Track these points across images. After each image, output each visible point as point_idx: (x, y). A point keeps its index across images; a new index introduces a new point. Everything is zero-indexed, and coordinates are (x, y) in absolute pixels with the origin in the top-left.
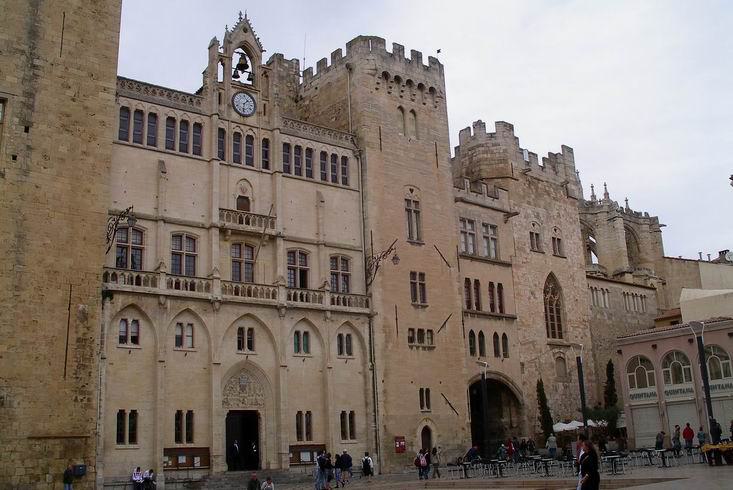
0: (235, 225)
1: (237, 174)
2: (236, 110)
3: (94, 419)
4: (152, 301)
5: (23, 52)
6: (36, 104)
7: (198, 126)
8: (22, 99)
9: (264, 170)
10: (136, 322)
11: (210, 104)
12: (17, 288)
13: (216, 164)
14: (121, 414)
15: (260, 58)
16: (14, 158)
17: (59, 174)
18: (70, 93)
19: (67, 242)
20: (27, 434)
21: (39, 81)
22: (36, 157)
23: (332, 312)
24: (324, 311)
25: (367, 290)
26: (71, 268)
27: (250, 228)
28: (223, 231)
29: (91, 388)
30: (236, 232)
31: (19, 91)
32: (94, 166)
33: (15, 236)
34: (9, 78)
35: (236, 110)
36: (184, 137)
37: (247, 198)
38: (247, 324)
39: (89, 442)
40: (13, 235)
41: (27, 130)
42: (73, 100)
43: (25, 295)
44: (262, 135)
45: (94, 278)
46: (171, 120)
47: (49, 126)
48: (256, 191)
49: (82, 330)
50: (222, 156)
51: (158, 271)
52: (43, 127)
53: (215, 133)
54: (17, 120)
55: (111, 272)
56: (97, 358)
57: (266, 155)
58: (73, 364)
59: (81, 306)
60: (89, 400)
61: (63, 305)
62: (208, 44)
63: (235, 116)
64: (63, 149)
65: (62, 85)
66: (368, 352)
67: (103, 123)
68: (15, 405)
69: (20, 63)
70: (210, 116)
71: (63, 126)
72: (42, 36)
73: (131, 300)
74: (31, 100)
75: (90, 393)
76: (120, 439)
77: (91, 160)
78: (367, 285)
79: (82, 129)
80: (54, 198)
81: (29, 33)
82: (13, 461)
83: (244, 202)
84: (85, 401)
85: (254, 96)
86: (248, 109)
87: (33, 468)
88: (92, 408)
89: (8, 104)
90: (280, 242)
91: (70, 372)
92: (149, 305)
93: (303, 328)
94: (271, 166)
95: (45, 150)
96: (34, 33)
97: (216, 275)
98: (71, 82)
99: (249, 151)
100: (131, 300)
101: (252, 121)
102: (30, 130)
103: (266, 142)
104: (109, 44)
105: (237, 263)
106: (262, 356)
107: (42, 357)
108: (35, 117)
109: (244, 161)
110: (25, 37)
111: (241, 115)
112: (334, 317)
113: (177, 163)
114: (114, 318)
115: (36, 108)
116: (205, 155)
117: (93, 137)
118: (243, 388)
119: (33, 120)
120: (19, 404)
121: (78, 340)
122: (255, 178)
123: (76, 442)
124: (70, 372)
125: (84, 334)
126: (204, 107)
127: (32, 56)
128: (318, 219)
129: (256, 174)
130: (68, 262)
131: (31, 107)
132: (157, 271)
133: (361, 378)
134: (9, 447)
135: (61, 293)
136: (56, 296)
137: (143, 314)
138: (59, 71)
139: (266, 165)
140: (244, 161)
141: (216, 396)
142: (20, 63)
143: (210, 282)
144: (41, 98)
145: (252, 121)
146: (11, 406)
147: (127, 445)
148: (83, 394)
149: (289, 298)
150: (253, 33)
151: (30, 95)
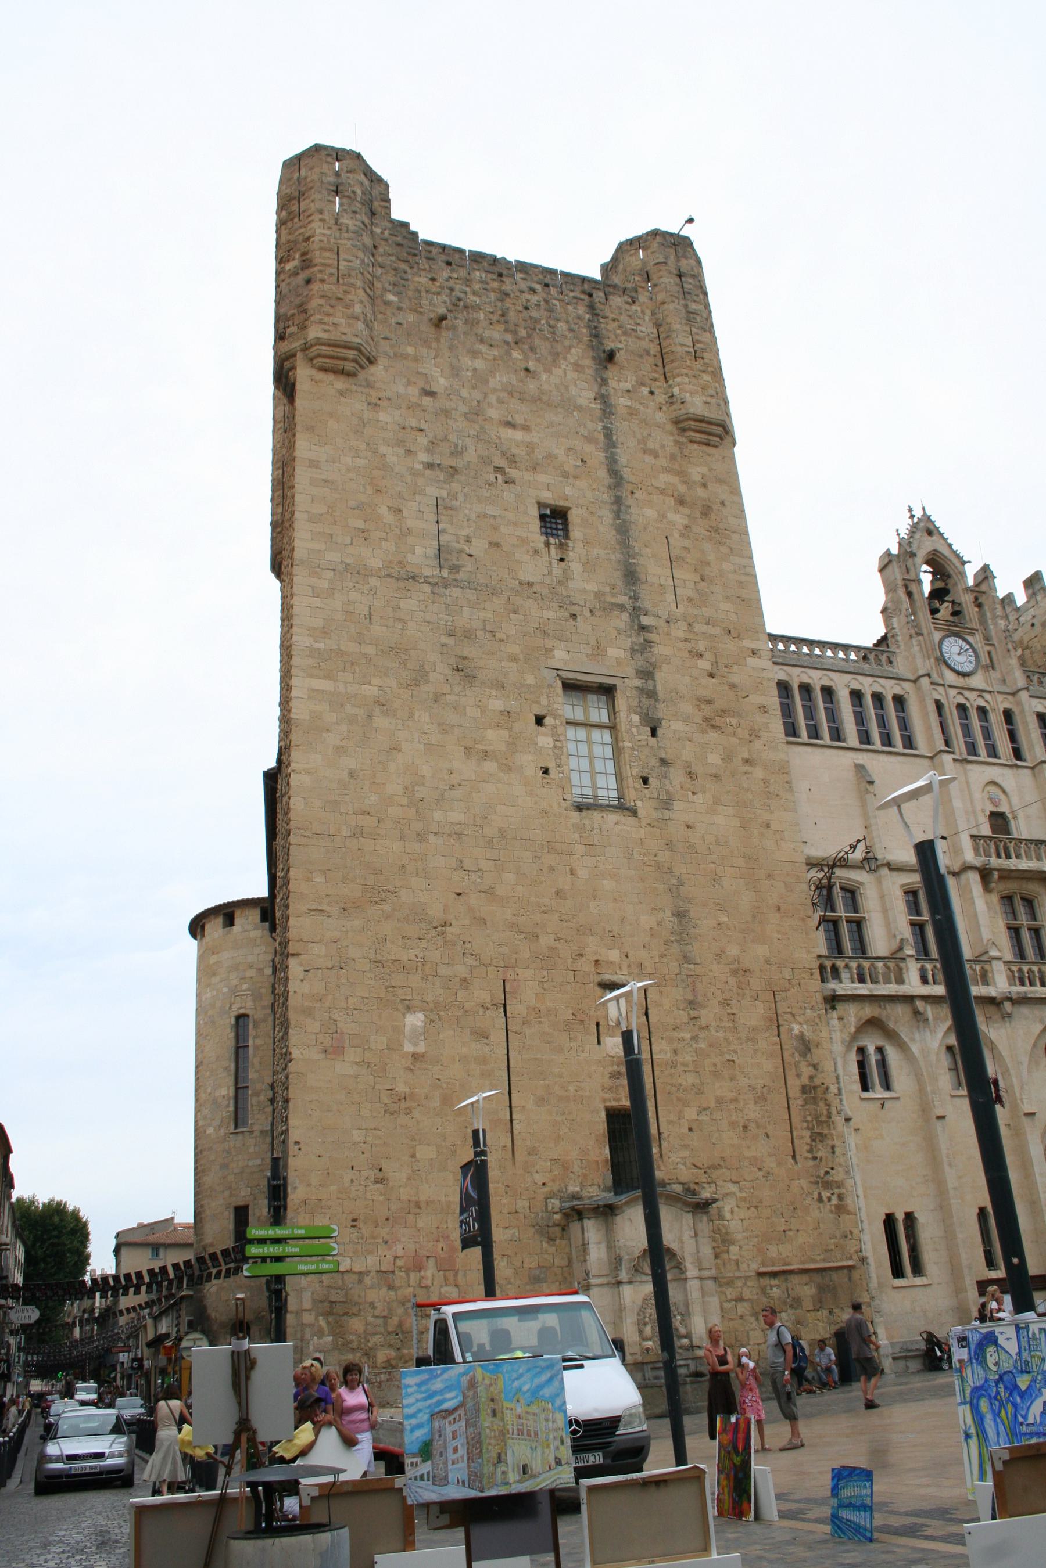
0: (1000, 861)
1: (980, 774)
2: (949, 666)
3: (856, 1232)
5: (622, 607)
6: (659, 688)
7: (899, 701)
8: (638, 683)
9: (1019, 763)
10: (880, 1050)
11: (910, 659)
12: (692, 1004)
13: (947, 758)
14: (889, 1221)
15: (963, 575)
16: (645, 781)
17: (717, 802)
18: (704, 665)
19: (754, 917)
20: (754, 1266)
21: (655, 650)
22: (677, 776)
26: (767, 961)
27: (1025, 864)
28: (985, 874)
29: (838, 1175)
30: (1007, 875)
31: (630, 671)
32: (765, 782)
33: (673, 915)
34: (614, 652)
35: (949, 666)
36: (882, 721)
37: (1002, 815)
39: (856, 1275)
40: (667, 915)
41: (654, 733)
42: (712, 676)
43: (707, 1015)
44: (998, 705)
45: (806, 976)
46: (856, 695)
47: (686, 720)
48: (1015, 800)
49: (806, 1071)
50: (947, 743)
51: (899, 955)
52: (677, 726)
53: (932, 708)
54: (636, 718)
55: (828, 964)
56: (839, 1120)
57: (1012, 736)
58: (804, 1136)
59: (796, 1029)
60: (840, 1197)
61: (768, 1028)
62: (876, 566)
63: (950, 677)
64: (714, 758)
65: (690, 652)
67: (763, 709)
68: (728, 1216)
69: (622, 626)
70: (914, 681)
71: (706, 719)
72: (642, 577)
73: (869, 1011)
74: (650, 682)
75: (839, 1185)
76: (897, 1271)
77: (758, 773)
79: (734, 721)
80: (718, 843)
81: (625, 576)
82: (741, 1317)
83: (999, 820)
84: (835, 1201)
85: (969, 638)
86: (964, 661)
88: (849, 1213)
89: (619, 694)
91: (802, 1148)
92: (897, 1016)
94: (1026, 752)
95: (688, 765)
96: (631, 576)
97: (994, 953)
98: (701, 646)
99: (987, 733)
100: (869, 1011)
101: (977, 681)
102: (660, 731)
103: (1008, 715)
104: (743, 578)
105: (1015, 932)
107: (752, 1125)
108: (662, 711)
109: (982, 750)
110: (620, 583)
111: (959, 673)
113: (878, 764)
115: (661, 695)
116: (923, 748)
117: (754, 734)
119: (660, 715)
120: (732, 1212)
121: (804, 1089)
122: (1008, 778)
123: (834, 1279)
124: (802, 1148)
125: (811, 1078)
126: (901, 667)
127: (636, 612)
129: (1007, 771)
130: (761, 951)
131: (652, 694)
132: (896, 956)
135: (760, 1009)
136: (753, 1015)
137: (891, 1035)
138: (679, 631)
139: (1018, 754)
140: (982, 750)
142: (622, 626)
143: (987, 967)
144: (663, 679)
145: (977, 681)
146: (721, 1217)
147: (910, 1280)
148: (828, 1185)
150: (941, 534)
151: (647, 674)
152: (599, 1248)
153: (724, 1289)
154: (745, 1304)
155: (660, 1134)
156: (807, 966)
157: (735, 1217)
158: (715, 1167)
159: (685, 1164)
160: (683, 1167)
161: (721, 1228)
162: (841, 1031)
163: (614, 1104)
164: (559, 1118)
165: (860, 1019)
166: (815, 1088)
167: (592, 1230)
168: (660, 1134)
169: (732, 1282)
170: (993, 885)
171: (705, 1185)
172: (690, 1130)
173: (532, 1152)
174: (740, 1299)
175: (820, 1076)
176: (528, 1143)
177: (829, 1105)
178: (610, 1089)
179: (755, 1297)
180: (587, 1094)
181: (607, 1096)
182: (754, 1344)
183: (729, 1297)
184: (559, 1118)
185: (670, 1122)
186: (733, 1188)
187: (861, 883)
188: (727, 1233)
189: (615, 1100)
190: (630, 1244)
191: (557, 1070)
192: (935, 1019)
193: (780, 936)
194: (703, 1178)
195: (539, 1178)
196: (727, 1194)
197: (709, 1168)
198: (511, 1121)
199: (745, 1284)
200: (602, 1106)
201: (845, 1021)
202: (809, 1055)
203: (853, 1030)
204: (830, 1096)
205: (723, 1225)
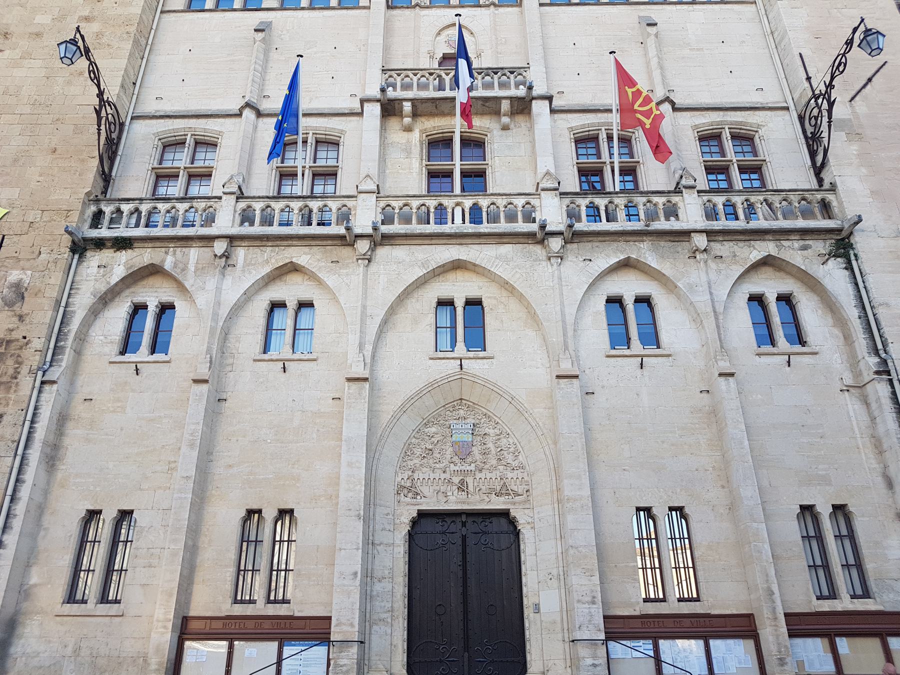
4: (194, 253)
23: (711, 234)
24: (685, 234)
25: (820, 181)
38: (460, 288)
56: (26, 383)
66: (857, 325)
78: (818, 170)
90: (540, 108)
93: (629, 287)
106: (515, 358)
112: (722, 248)
114: (106, 299)
118: (463, 452)
128: (648, 63)
133: (851, 404)
137: (181, 287)
141: (350, 464)
149: (573, 215)
156: (65, 207)
162: (96, 280)
165: (132, 266)
166: (9, 342)
170: (407, 120)
175: (21, 327)
177: (20, 363)
187: (220, 133)
192: (247, 264)
193: (40, 179)
201: (108, 269)
202: (19, 304)
203: (115, 279)
204: (27, 353)
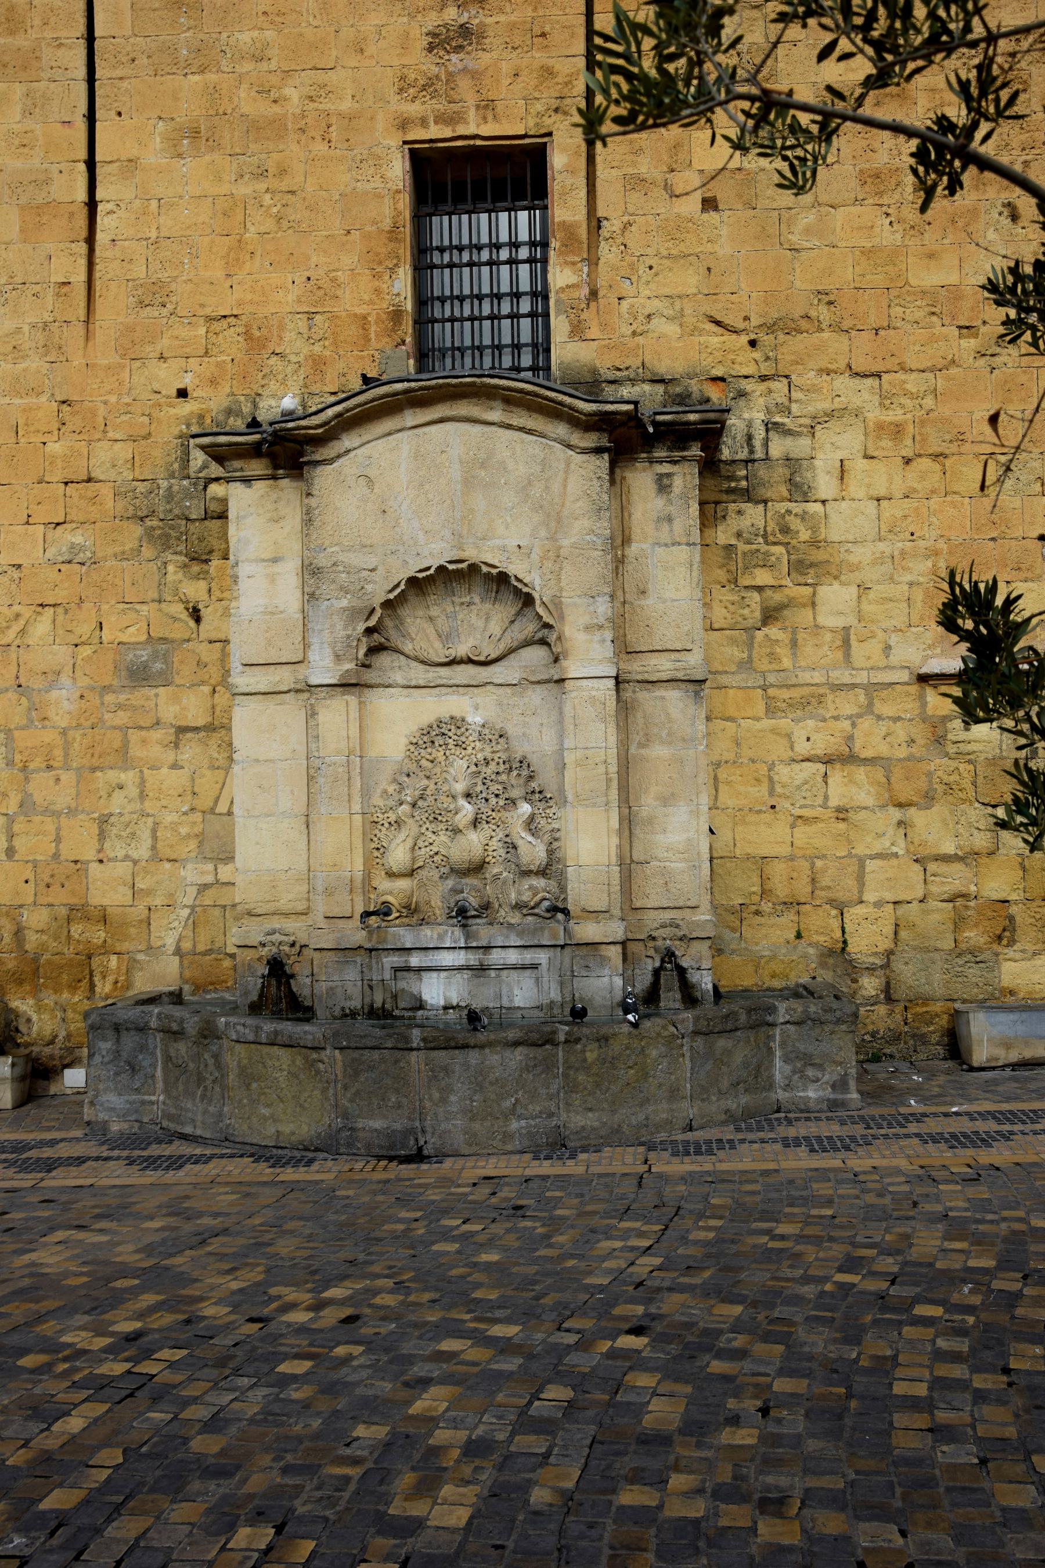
68: (825, 485)
82: (842, 813)
87: (966, 857)
134: (813, 735)
146: (799, 490)
152: (272, 579)
153: (784, 723)
154: (861, 773)
155: (595, 223)
157: (855, 488)
158: (783, 326)
159: (678, 317)
160: (672, 329)
161: (795, 524)
163: (435, 132)
164: (244, 189)
167: (257, 514)
168: (595, 223)
169: (821, 699)
171: (748, 386)
172: (709, 204)
173: (153, 295)
174: (844, 758)
176: (139, 271)
178: (428, 86)
179: (902, 753)
180: (346, 105)
181: (414, 109)
182: (879, 904)
183: (802, 748)
184: (244, 189)
185: (636, 183)
186: (859, 394)
188: (815, 543)
189: (441, 119)
190: (356, 559)
191: (245, 37)
194: (747, 362)
195: (169, 377)
196: (830, 415)
197: (771, 328)
198: (92, 205)
199: (869, 708)
200: (394, 141)
205: (803, 517)
